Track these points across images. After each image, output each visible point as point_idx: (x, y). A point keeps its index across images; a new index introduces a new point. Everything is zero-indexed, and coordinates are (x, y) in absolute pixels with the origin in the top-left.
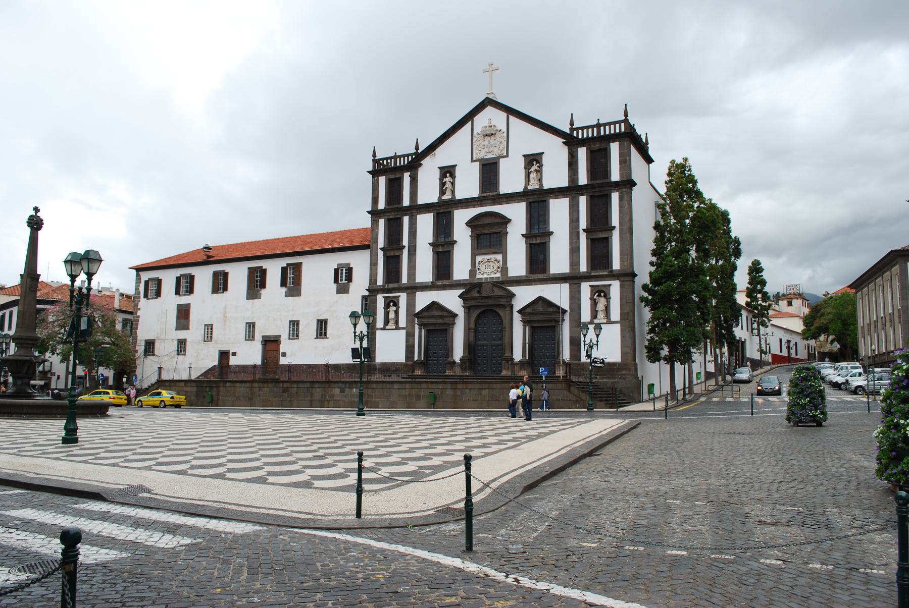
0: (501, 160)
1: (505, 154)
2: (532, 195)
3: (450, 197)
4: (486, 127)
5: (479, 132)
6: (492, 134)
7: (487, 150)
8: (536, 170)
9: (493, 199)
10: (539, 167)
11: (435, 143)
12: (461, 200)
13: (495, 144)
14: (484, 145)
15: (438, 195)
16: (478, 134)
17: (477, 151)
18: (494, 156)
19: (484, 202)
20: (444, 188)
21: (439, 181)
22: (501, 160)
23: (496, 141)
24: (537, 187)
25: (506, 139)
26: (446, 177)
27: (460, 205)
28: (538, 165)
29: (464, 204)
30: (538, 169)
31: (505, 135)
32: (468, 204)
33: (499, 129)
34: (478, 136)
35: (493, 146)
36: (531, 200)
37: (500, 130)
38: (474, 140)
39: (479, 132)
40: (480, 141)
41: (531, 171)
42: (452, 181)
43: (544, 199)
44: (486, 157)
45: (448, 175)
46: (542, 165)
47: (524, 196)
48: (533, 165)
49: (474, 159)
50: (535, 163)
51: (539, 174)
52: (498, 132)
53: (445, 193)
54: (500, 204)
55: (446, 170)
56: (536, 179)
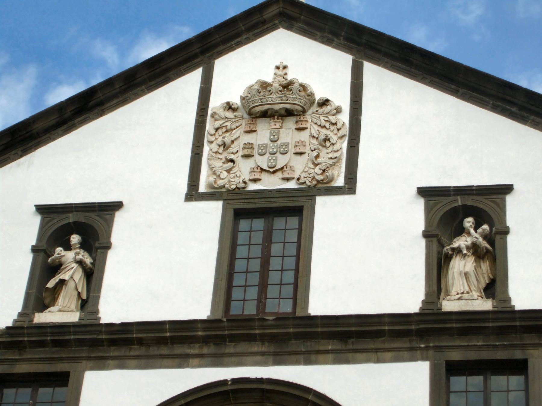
0: (321, 202)
1: (340, 182)
2: (464, 332)
3: (74, 317)
4: (264, 85)
5: (236, 101)
6: (289, 113)
7: (263, 162)
8: (475, 248)
9: (273, 339)
10: (489, 238)
11: (40, 125)
12: (126, 327)
13: (302, 144)
14: (249, 146)
15: (18, 307)
16: (229, 107)
17: (217, 164)
18: (292, 185)
19: (230, 349)
20: (51, 284)
21: (29, 258)
22: (321, 202)
23: (304, 136)
24: (487, 305)
25: (346, 131)
26: (68, 247)
27: (114, 352)
28: (485, 227)
29: (136, 351)
30: (485, 244)
31: (345, 118)
32: (154, 350)
33: (319, 96)
34: (230, 114)
35: (292, 150)
36: (455, 356)
37: (325, 103)
38: (209, 126)
39: (236, 101)
40: (236, 133)
41: (458, 251)
42: (88, 260)
43: (518, 355)
44: (252, 187)
45: (75, 239)
46: (506, 231)
47: (422, 334)
48: (461, 231)
49: (202, 188)
50: (469, 222)
51: (485, 266)
52: (314, 108)
53: (54, 301)
54: (308, 362)
55: (71, 218)
56: (473, 279)
